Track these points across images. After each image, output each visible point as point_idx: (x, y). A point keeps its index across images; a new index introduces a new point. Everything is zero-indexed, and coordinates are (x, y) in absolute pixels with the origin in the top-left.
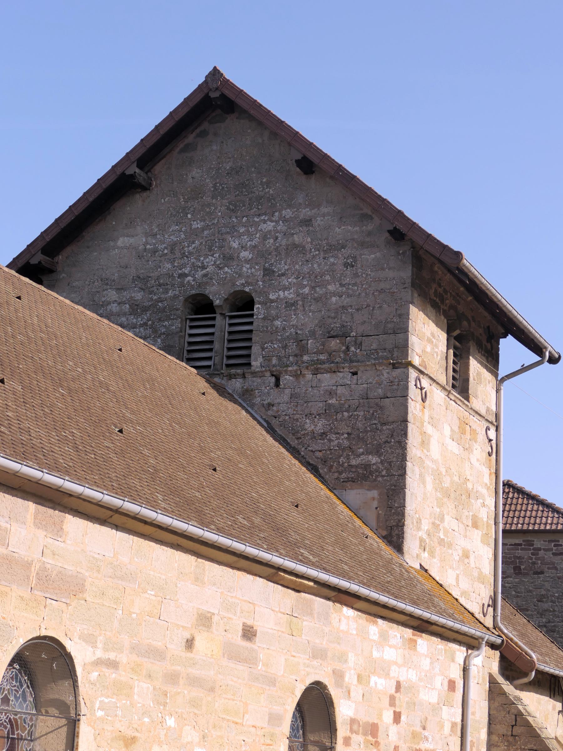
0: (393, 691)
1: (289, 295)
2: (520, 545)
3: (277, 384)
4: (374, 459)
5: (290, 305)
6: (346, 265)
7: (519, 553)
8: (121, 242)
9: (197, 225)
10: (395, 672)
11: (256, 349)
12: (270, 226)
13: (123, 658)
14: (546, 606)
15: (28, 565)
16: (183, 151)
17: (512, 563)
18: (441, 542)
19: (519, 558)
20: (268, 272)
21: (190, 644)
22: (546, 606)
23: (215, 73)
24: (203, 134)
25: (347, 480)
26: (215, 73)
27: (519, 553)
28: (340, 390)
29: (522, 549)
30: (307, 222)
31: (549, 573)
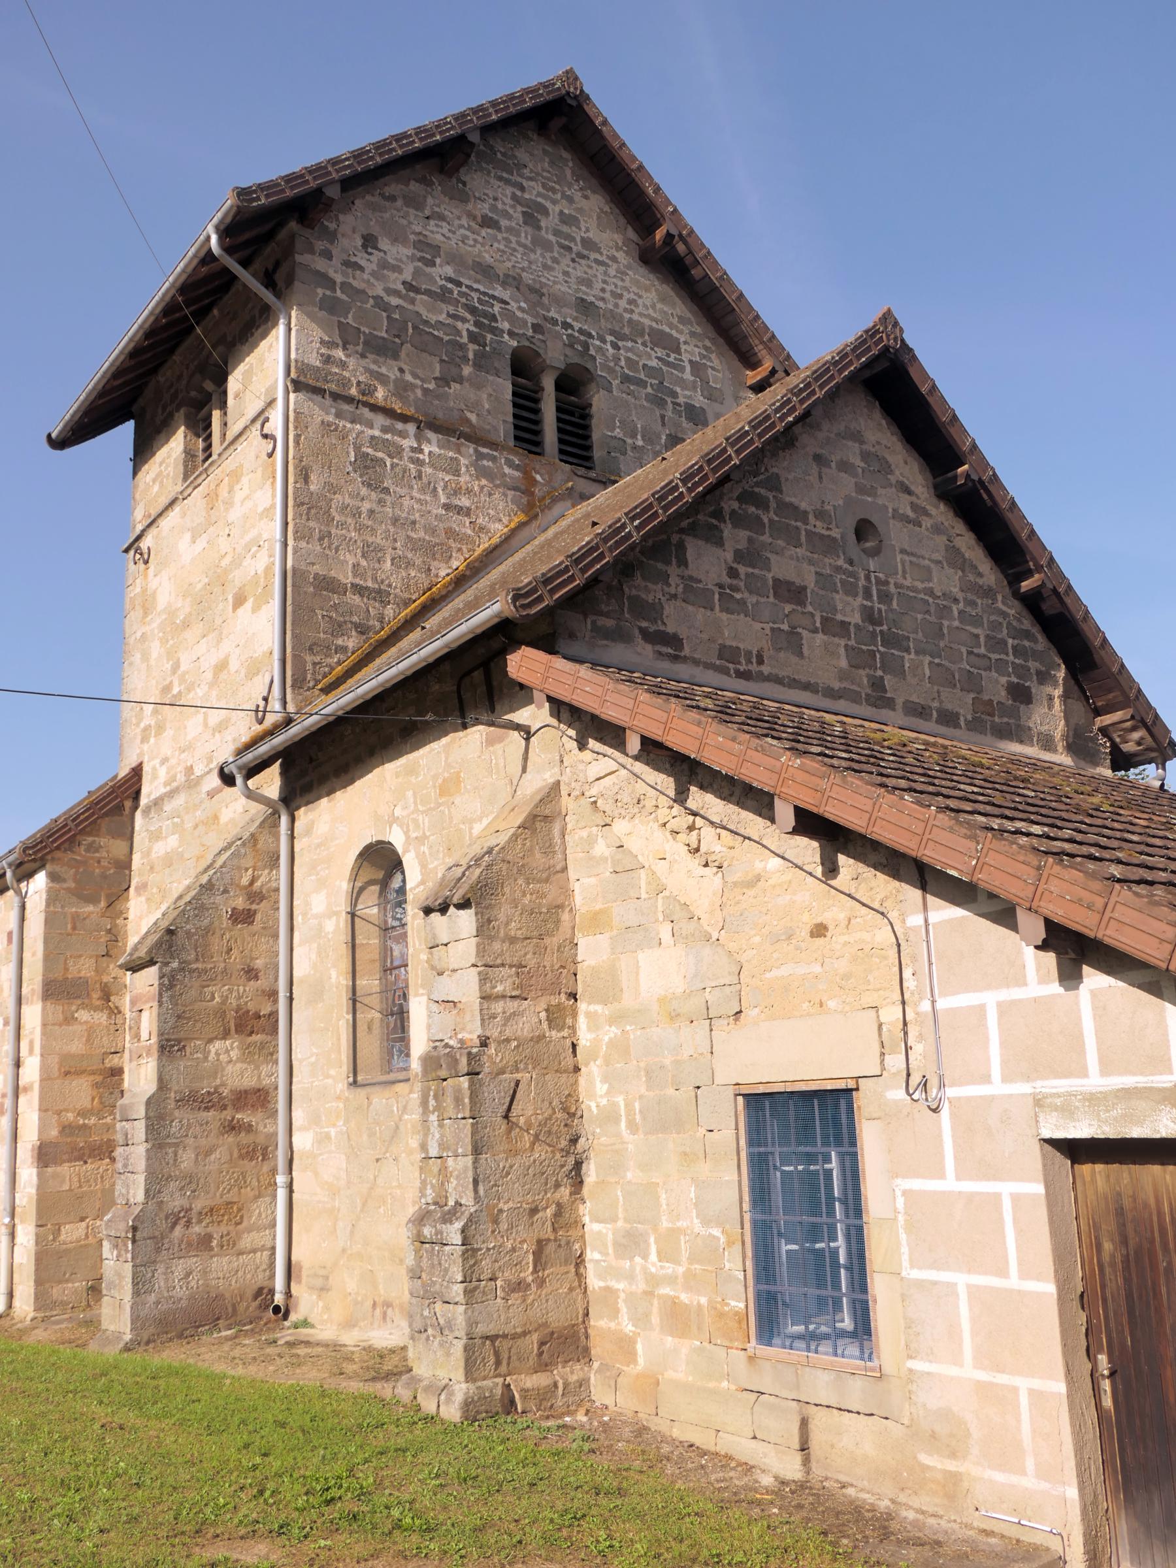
23: (570, 76)
26: (570, 76)
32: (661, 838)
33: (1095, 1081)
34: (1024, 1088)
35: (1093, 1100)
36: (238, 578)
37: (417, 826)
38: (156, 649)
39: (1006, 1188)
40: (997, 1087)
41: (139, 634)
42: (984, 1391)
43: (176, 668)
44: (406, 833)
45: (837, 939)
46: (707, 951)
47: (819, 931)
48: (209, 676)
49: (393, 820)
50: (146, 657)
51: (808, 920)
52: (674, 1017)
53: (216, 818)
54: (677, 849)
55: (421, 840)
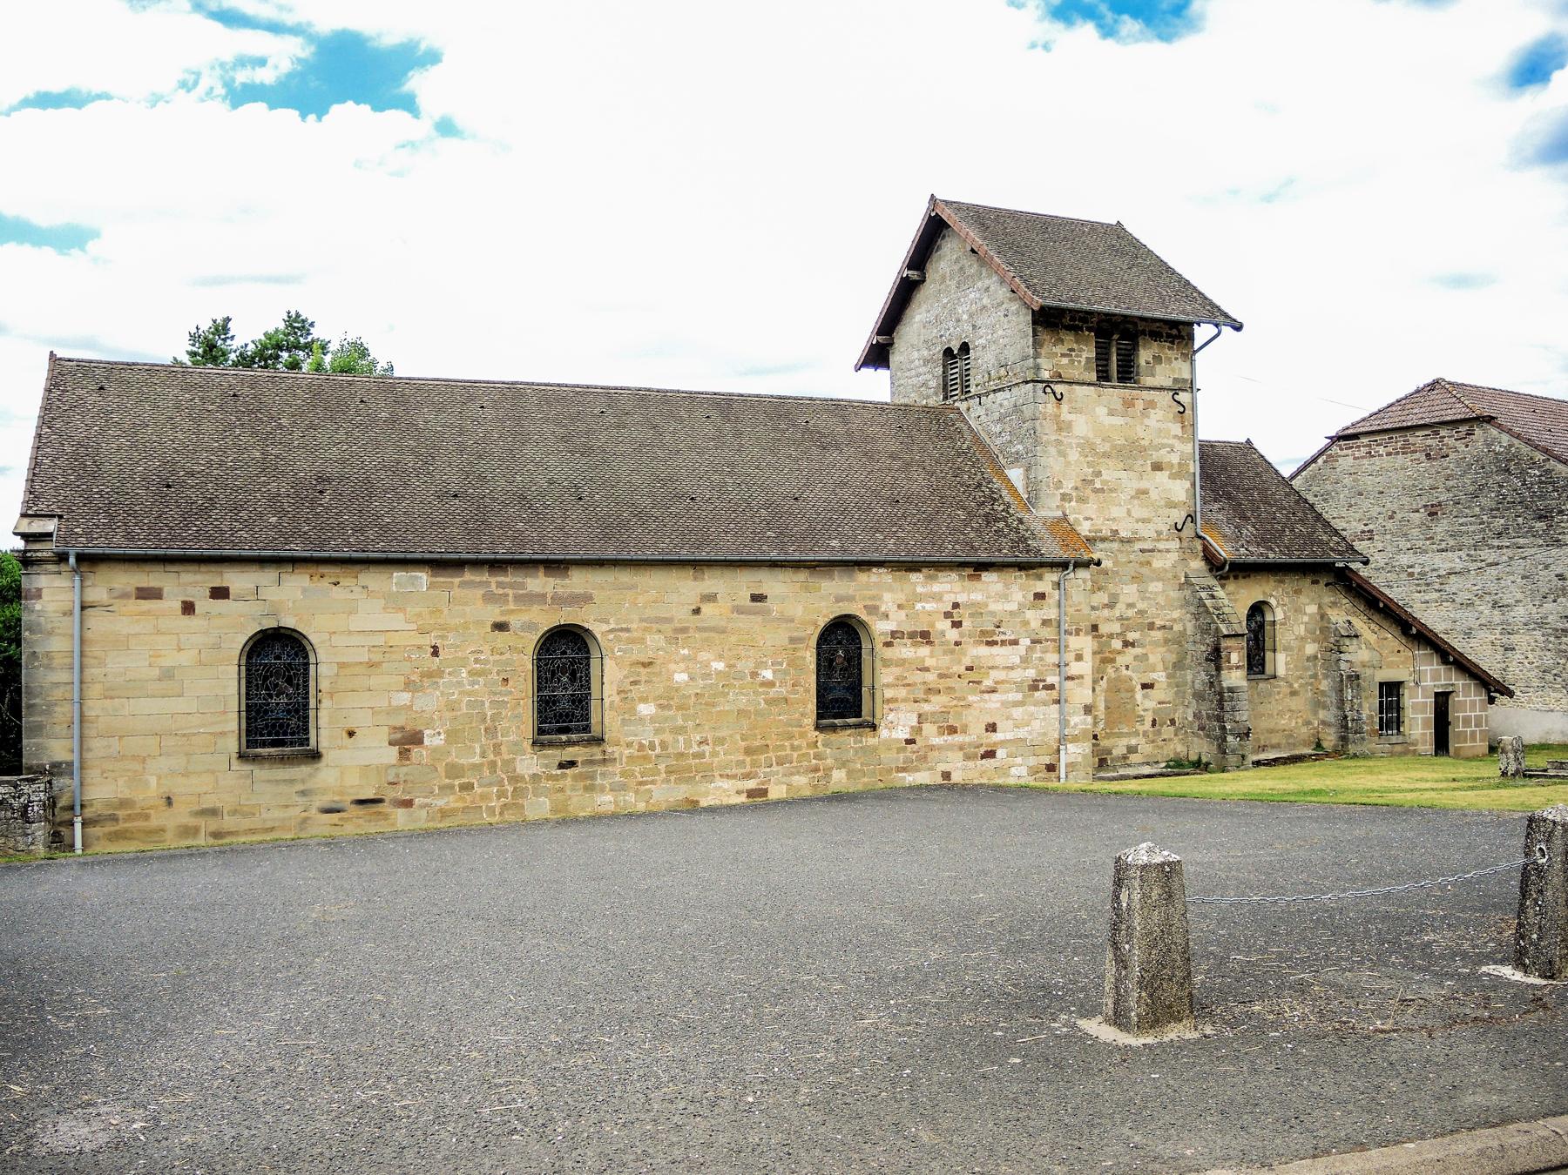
0: (949, 609)
1: (982, 341)
2: (1430, 435)
3: (980, 404)
4: (1020, 447)
5: (984, 347)
6: (1006, 316)
7: (1429, 442)
8: (917, 318)
9: (945, 301)
10: (946, 597)
11: (972, 382)
12: (972, 296)
13: (634, 626)
14: (1451, 483)
15: (544, 596)
16: (937, 251)
17: (1424, 451)
18: (1096, 491)
19: (1429, 446)
20: (974, 326)
21: (697, 611)
22: (1451, 483)
24: (944, 237)
25: (1012, 462)
27: (1429, 442)
28: (1005, 403)
29: (1431, 439)
30: (987, 289)
31: (1452, 456)
32: (1361, 624)
33: (1443, 682)
34: (1432, 683)
35: (1442, 685)
36: (1156, 456)
37: (1283, 600)
38: (1074, 455)
39: (1429, 700)
40: (1429, 683)
41: (1053, 438)
42: (1422, 734)
43: (1099, 474)
44: (1278, 601)
45: (1402, 653)
46: (1375, 652)
47: (1399, 651)
48: (1133, 493)
49: (1271, 596)
50: (1063, 454)
51: (1396, 649)
52: (1364, 666)
53: (1149, 563)
54: (1366, 627)
55: (1284, 605)
